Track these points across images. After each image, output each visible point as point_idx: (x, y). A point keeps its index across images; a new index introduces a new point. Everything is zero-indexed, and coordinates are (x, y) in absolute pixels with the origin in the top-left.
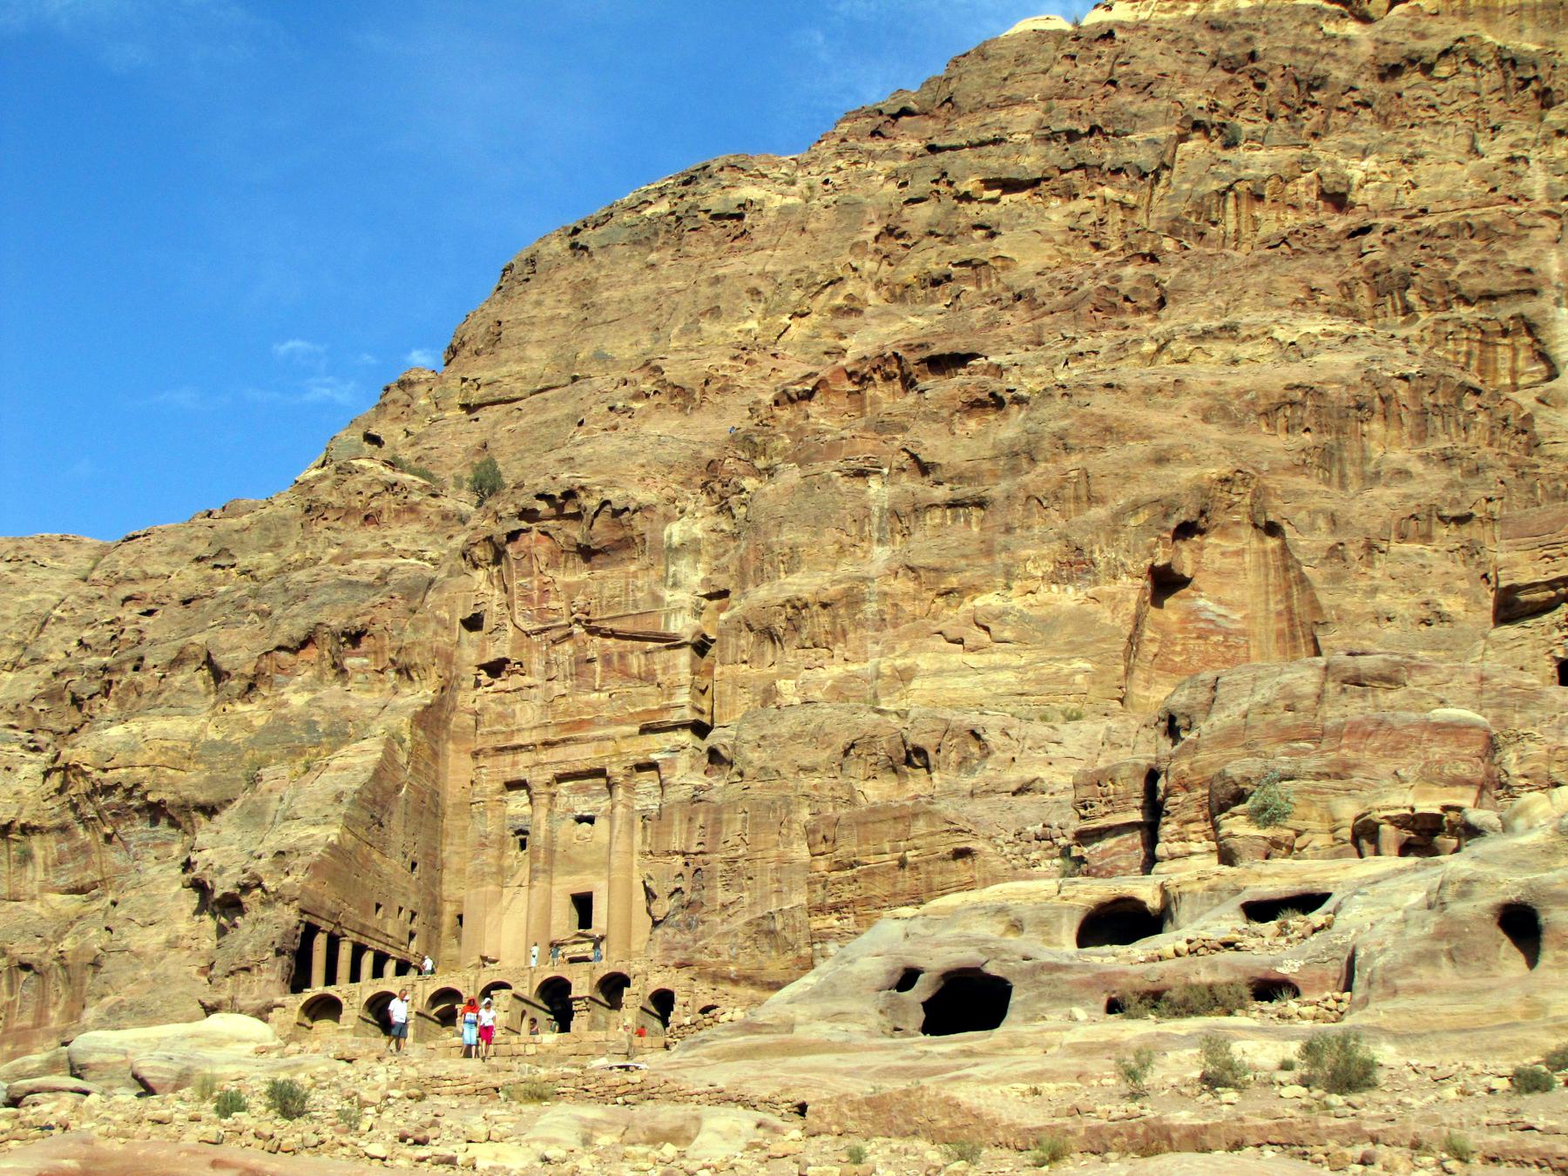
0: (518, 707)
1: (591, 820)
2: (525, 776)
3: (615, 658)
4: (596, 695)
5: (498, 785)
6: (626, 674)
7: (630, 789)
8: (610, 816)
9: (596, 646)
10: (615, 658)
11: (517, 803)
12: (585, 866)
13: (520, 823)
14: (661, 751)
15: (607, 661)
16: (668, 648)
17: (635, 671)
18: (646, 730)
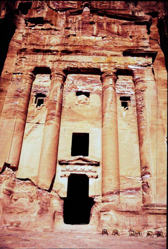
0: (47, 37)
1: (87, 94)
2: (50, 65)
3: (105, 25)
4: (94, 37)
5: (32, 68)
6: (110, 32)
7: (115, 81)
8: (102, 94)
9: (95, 18)
10: (105, 25)
11: (42, 81)
12: (84, 118)
13: (41, 90)
14: (136, 64)
15: (100, 26)
16: (136, 24)
17: (116, 30)
18: (128, 53)
